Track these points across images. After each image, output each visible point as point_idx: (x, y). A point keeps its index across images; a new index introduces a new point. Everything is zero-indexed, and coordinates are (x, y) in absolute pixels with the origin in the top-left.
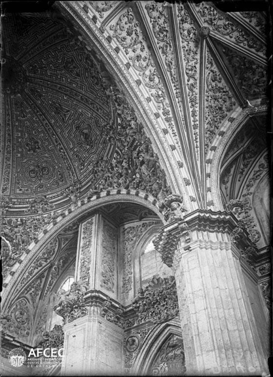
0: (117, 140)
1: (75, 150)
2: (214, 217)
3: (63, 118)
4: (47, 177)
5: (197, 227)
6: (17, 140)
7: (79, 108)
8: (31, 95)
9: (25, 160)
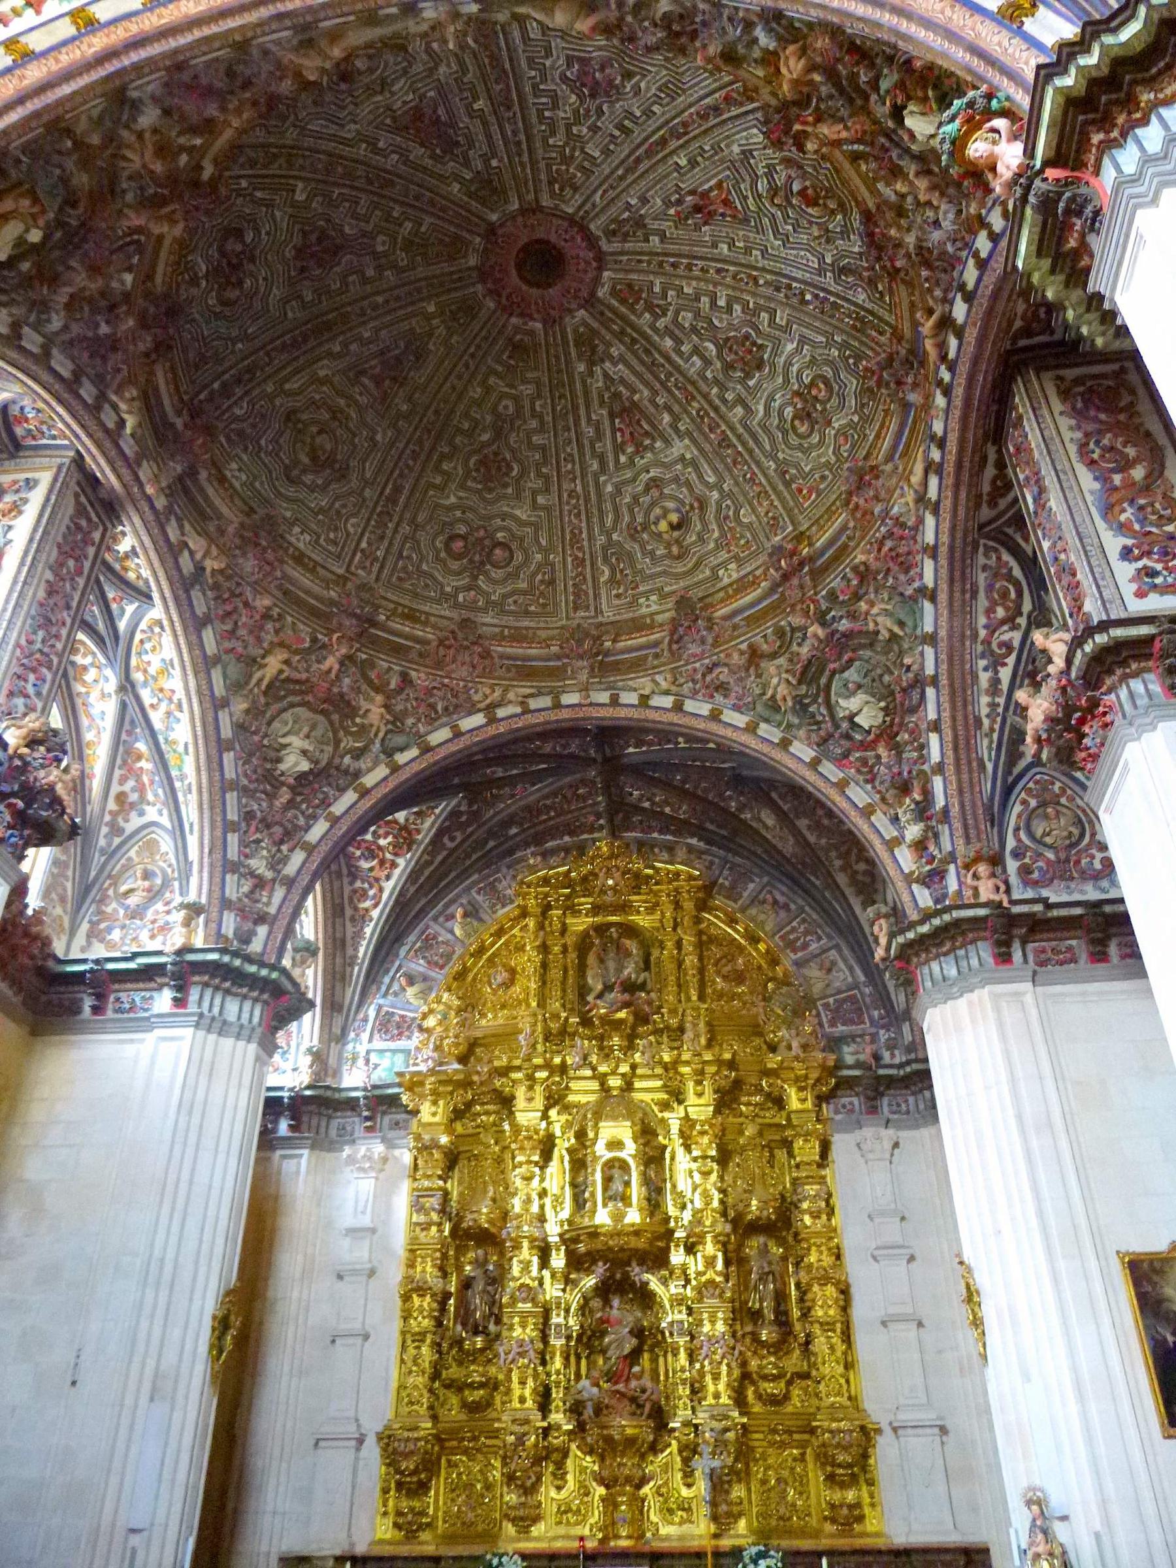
0: (814, 125)
1: (828, 260)
2: (1125, 35)
3: (734, 217)
4: (834, 401)
5: (1096, 138)
6: (705, 379)
7: (727, 146)
8: (627, 245)
9: (761, 408)
